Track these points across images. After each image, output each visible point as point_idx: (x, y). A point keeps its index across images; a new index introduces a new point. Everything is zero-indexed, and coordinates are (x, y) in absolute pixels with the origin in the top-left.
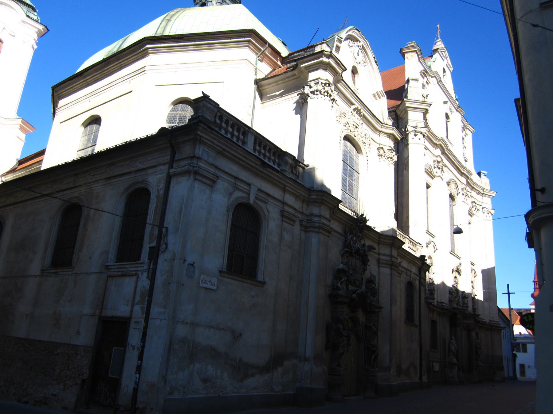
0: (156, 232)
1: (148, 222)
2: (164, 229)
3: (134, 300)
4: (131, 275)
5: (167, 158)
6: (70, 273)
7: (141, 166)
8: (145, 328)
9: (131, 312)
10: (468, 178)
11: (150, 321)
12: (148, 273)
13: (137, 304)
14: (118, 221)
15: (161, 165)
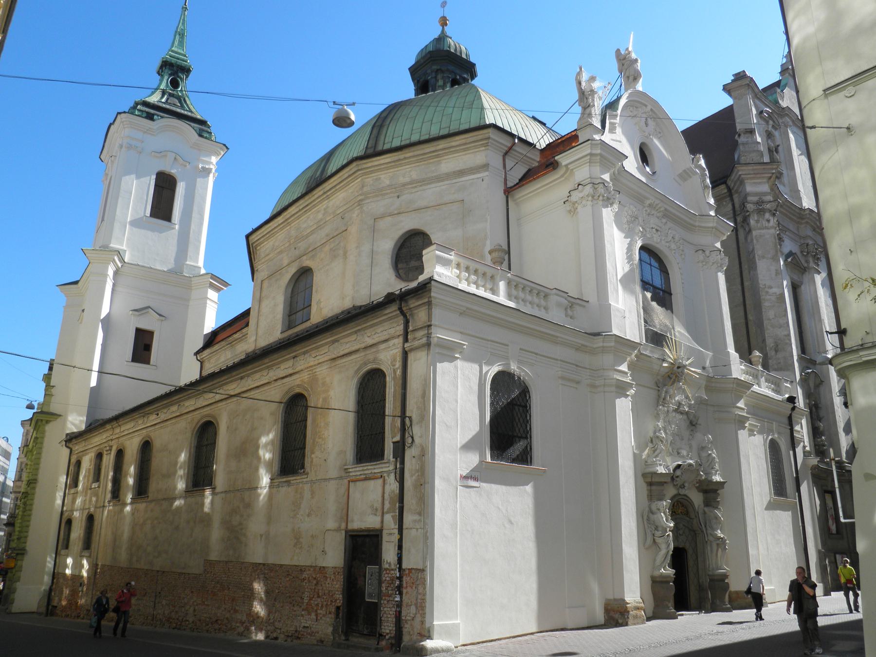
1: (387, 413)
2: (407, 420)
3: (383, 508)
5: (400, 329)
7: (370, 341)
8: (400, 541)
9: (382, 522)
11: (405, 532)
13: (387, 513)
14: (351, 418)
15: (393, 338)
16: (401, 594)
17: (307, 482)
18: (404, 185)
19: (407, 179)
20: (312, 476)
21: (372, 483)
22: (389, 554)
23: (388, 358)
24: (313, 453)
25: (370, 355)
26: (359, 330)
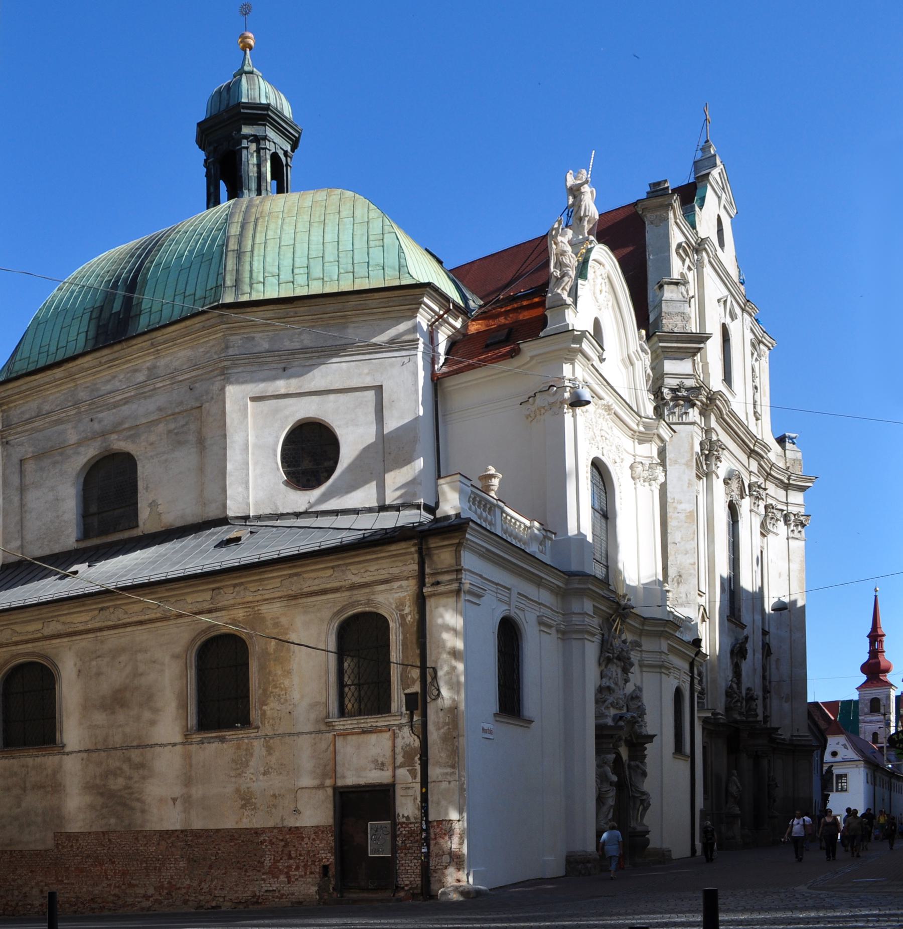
0: (416, 673)
4: (381, 732)
6: (252, 735)
7: (357, 579)
9: (394, 776)
10: (762, 457)
12: (411, 727)
13: (400, 767)
16: (428, 846)
17: (256, 738)
18: (293, 353)
19: (297, 345)
20: (267, 730)
21: (373, 737)
22: (407, 807)
23: (392, 600)
24: (263, 703)
25: (360, 595)
26: (339, 566)
